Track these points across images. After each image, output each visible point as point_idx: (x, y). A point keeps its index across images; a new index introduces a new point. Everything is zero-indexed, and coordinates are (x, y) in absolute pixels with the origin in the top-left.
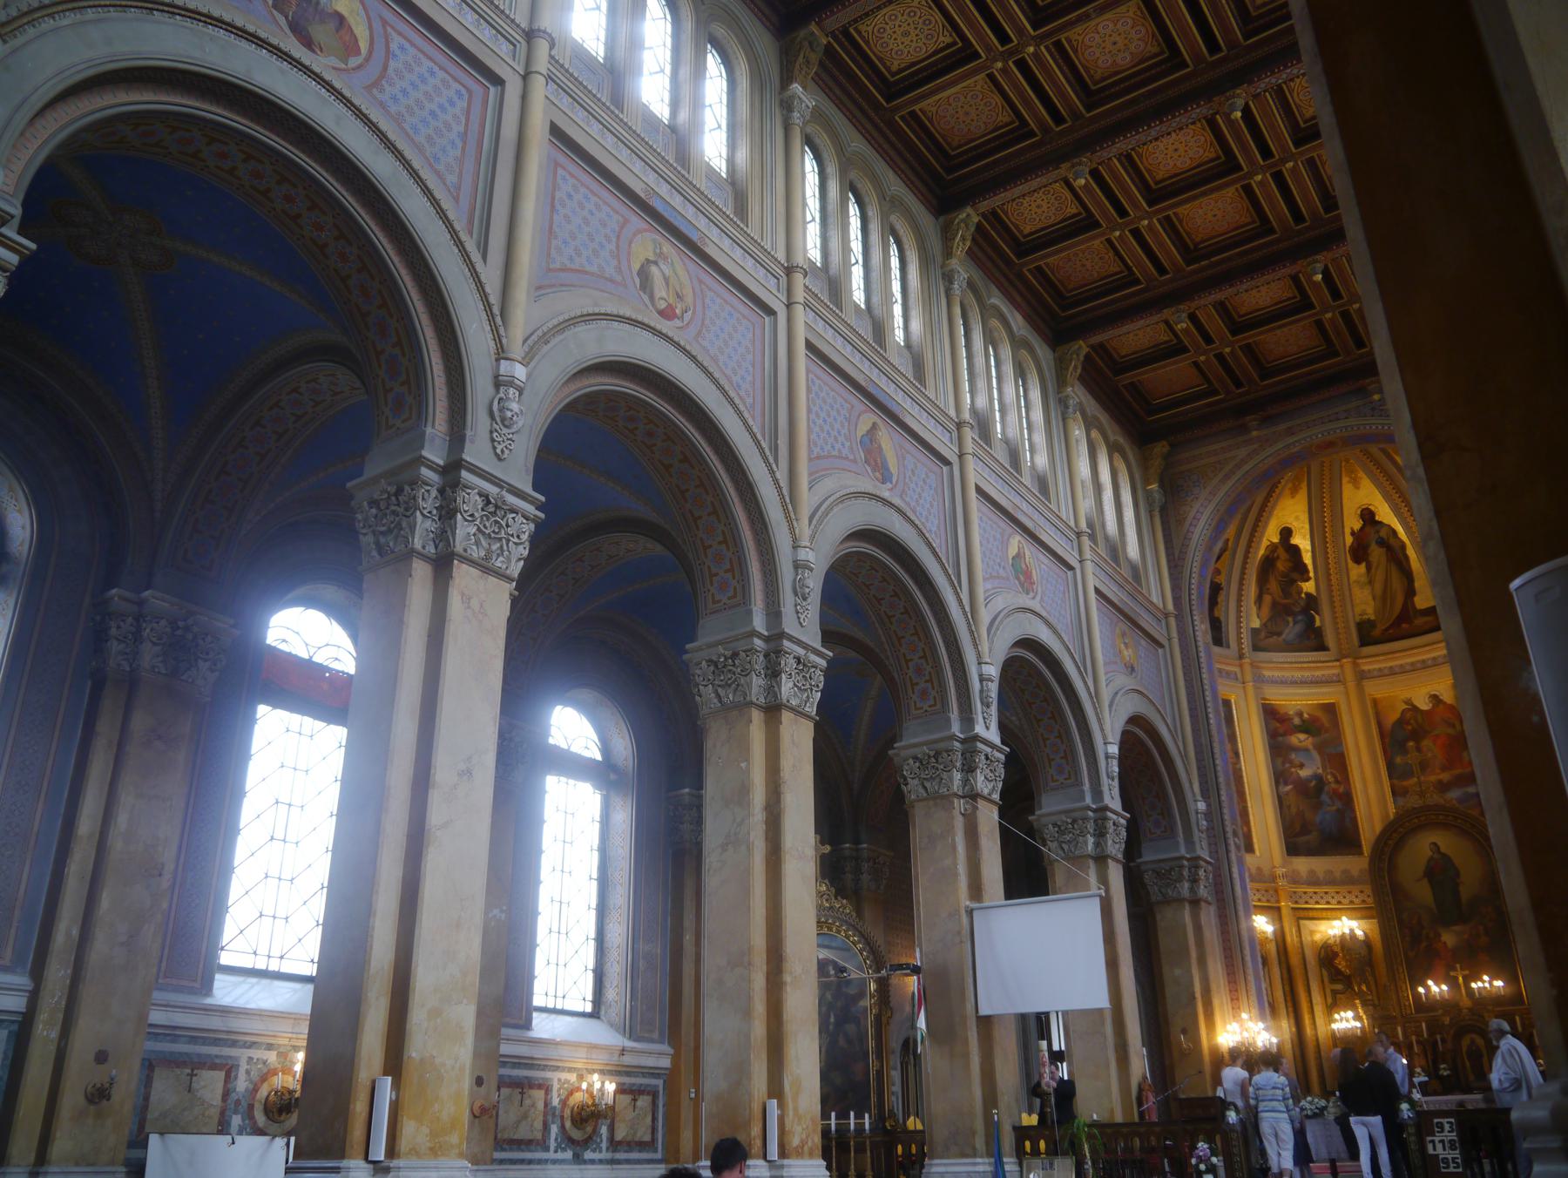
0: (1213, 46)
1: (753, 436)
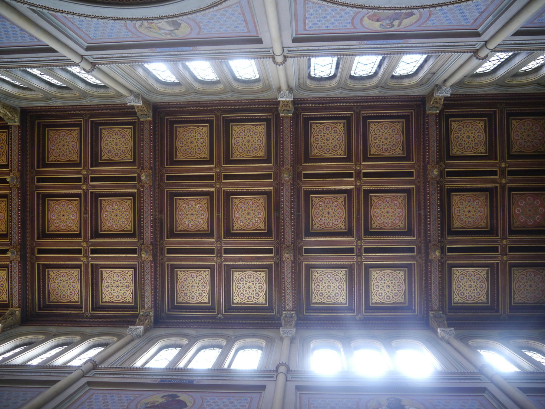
0: (40, 251)
1: (56, 11)
